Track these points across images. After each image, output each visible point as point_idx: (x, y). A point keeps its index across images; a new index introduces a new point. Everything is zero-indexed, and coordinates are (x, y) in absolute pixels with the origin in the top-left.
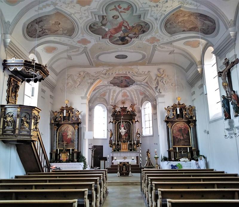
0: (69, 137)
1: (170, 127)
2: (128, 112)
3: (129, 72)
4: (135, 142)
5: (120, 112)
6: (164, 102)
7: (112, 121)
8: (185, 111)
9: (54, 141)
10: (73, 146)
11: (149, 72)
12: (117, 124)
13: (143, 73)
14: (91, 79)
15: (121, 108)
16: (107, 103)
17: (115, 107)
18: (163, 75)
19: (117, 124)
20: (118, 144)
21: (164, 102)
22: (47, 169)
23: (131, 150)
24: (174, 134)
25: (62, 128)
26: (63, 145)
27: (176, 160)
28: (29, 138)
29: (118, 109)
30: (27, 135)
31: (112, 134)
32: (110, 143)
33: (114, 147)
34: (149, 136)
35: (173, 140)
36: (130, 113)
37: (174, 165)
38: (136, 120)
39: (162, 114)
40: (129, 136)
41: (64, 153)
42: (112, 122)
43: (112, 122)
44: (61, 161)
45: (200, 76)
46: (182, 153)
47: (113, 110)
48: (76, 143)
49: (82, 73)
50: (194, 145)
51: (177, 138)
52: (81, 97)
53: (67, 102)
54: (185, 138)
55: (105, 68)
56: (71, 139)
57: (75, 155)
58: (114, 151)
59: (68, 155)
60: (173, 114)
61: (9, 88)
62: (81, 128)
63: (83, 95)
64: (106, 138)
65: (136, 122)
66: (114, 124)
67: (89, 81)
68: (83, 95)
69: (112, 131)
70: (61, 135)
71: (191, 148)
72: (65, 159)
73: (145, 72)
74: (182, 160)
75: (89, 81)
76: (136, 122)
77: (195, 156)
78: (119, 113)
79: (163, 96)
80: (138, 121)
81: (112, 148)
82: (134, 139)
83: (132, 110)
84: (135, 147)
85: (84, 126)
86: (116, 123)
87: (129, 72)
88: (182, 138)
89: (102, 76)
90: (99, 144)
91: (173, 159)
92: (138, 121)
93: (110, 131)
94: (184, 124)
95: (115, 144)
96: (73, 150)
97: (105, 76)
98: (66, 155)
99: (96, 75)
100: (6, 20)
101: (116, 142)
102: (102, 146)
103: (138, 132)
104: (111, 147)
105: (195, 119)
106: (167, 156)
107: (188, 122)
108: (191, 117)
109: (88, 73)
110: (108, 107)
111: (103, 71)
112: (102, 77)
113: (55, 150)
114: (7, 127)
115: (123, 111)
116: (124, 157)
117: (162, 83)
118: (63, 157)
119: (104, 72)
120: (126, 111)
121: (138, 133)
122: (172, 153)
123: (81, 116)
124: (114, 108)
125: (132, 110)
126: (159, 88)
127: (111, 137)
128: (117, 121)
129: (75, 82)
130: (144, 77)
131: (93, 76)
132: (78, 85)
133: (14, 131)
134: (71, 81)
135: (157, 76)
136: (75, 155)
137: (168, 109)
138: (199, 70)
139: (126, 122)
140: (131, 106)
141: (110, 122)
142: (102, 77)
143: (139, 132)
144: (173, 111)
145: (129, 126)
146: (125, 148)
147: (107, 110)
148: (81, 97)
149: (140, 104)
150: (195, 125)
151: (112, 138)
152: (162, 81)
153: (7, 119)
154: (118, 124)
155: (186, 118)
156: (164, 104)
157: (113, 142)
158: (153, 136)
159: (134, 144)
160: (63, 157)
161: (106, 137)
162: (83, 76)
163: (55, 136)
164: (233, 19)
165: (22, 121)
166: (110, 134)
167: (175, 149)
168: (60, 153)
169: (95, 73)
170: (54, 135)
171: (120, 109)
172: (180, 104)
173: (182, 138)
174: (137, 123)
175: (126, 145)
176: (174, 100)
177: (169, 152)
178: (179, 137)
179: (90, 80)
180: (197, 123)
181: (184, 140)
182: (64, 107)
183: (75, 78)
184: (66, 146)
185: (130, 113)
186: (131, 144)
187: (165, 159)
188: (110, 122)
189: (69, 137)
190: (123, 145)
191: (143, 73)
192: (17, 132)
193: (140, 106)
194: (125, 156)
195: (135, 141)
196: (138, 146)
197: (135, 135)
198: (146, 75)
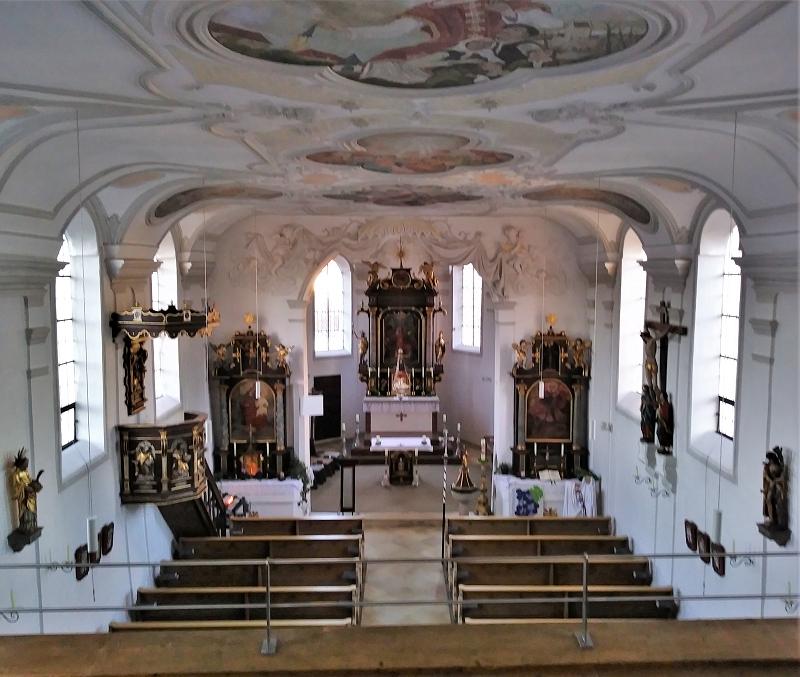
0: (262, 411)
1: (521, 394)
2: (415, 281)
3: (423, 234)
4: (432, 370)
5: (389, 281)
6: (513, 323)
7: (366, 307)
8: (565, 351)
9: (222, 423)
10: (272, 436)
11: (479, 234)
12: (380, 316)
13: (461, 238)
14: (314, 250)
15: (394, 270)
17: (375, 268)
18: (516, 245)
19: (380, 316)
20: (384, 375)
21: (513, 323)
22: (216, 510)
23: (418, 394)
24: (531, 410)
25: (241, 388)
26: (245, 434)
27: (529, 476)
28: (191, 493)
29: (384, 274)
30: (187, 490)
31: (366, 346)
32: (360, 372)
33: (373, 383)
34: (471, 354)
35: (528, 423)
37: (524, 489)
38: (436, 307)
39: (505, 354)
40: (415, 352)
41: (252, 455)
42: (368, 312)
44: (244, 477)
45: (613, 280)
46: (547, 458)
47: (370, 277)
48: (281, 429)
49: (288, 233)
50: (578, 439)
51: (538, 419)
52: (289, 301)
53: (249, 319)
54: (557, 418)
55: (354, 218)
56: (264, 416)
57: (279, 460)
58: (373, 394)
59: (262, 458)
60: (534, 359)
61: (127, 373)
62: (291, 387)
63: (294, 297)
67: (310, 255)
68: (294, 297)
69: (367, 336)
70: (238, 405)
71: (568, 446)
72: (253, 472)
73: (466, 235)
74: (545, 475)
75: (310, 255)
76: (435, 311)
77: (577, 467)
79: (511, 306)
80: (440, 310)
82: (429, 361)
83: (425, 278)
84: (429, 383)
85: (299, 382)
86: (377, 315)
87: (423, 234)
88: (550, 419)
89: (347, 240)
90: (329, 371)
91: (523, 474)
92: (440, 310)
93: (360, 336)
94: (559, 384)
95: (374, 374)
96: (273, 446)
97: (355, 242)
98: (255, 458)
99: (328, 239)
100: (109, 214)
102: (339, 377)
104: (362, 380)
105: (587, 374)
106: (509, 461)
107: (570, 382)
108: (580, 370)
109: (305, 232)
111: (347, 227)
112: (347, 246)
113: (227, 444)
114: (141, 476)
117: (512, 270)
118: (251, 465)
119: (352, 229)
121: (440, 345)
122: (523, 459)
123: (291, 355)
124: (374, 273)
125: (425, 278)
126: (501, 286)
127: (362, 356)
129: (268, 256)
130: (466, 249)
131: (320, 241)
132: (277, 266)
133: (158, 487)
134: (257, 254)
135: (500, 249)
136: (279, 460)
137: (520, 347)
138: (608, 266)
139: (406, 312)
141: (362, 310)
142: (347, 246)
143: (442, 341)
144: (534, 351)
145: (415, 323)
147: (352, 269)
148: (289, 301)
150: (587, 387)
151: (366, 357)
152: (511, 263)
153: (138, 459)
154: (383, 318)
155: (565, 369)
156: (511, 327)
157: (370, 370)
158: (480, 355)
159: (428, 374)
160: (251, 465)
161: (348, 350)
162: (292, 240)
163: (225, 410)
164: (688, 227)
165: (171, 460)
166: (360, 345)
167: (530, 446)
168: (239, 455)
169: (326, 233)
170: (221, 408)
172: (553, 334)
173: (550, 419)
174: (438, 314)
176: (539, 319)
177: (516, 455)
178: (542, 417)
179: (312, 253)
180: (592, 384)
181: (555, 422)
182: (242, 332)
183: (270, 244)
184: (253, 434)
186: (418, 375)
187: (505, 470)
188: (362, 310)
189: (262, 411)
191: (461, 238)
192: (165, 488)
195: (429, 367)
197: (430, 349)
198: (469, 243)
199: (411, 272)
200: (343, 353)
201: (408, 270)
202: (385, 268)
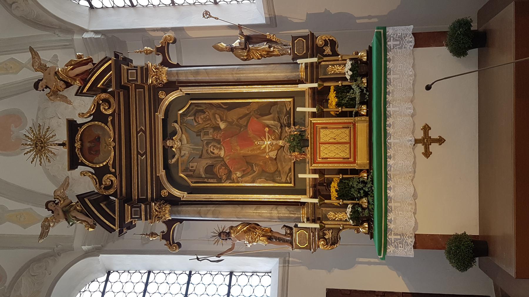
2: (98, 116)
12: (176, 193)
15: (73, 164)
16: (54, 255)
19: (176, 193)
36: (105, 101)
42: (170, 224)
43: (170, 224)
64: (277, 260)
65: (165, 63)
66: (179, 213)
78: (108, 179)
80: (162, 50)
81: (341, 234)
83: (74, 89)
86: (174, 202)
101: (303, 204)
103: (232, 49)
104: (334, 242)
110: (77, 244)
115: (98, 152)
116: (421, 148)
120: (99, 133)
125: (74, 89)
127: (271, 237)
128: (164, 193)
139: (168, 135)
140: (55, 94)
146: (343, 135)
149: (63, 36)
151: (278, 228)
171: (80, 168)
175: (325, 135)
185: (105, 101)
188: (166, 236)
190: (325, 152)
193: (76, 37)
194: (409, 139)
196: (333, 44)
199: (80, 121)
200: (276, 274)
201: (72, 126)
202: (66, 184)
